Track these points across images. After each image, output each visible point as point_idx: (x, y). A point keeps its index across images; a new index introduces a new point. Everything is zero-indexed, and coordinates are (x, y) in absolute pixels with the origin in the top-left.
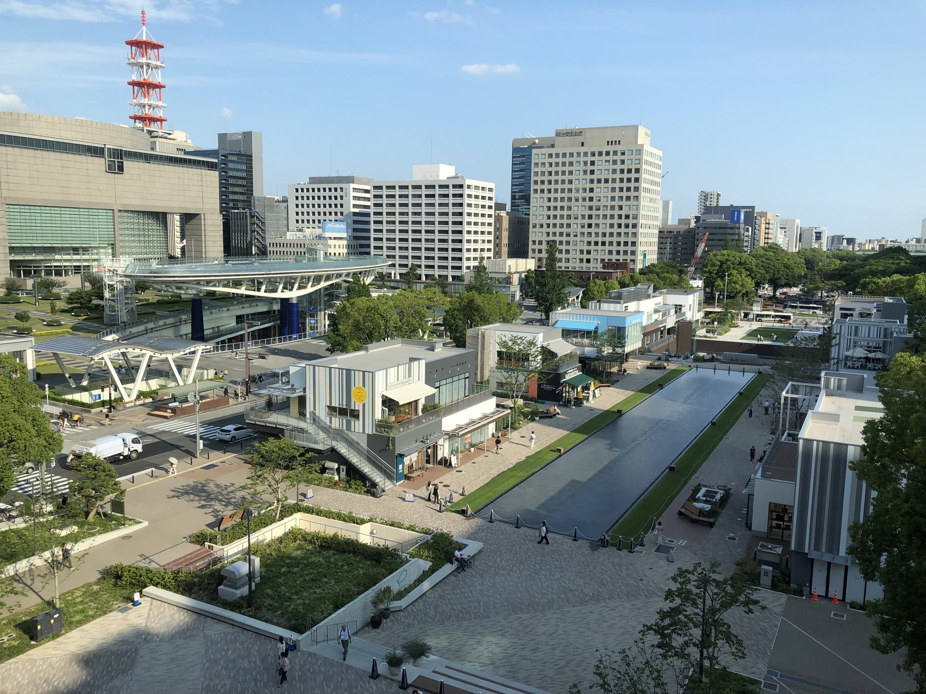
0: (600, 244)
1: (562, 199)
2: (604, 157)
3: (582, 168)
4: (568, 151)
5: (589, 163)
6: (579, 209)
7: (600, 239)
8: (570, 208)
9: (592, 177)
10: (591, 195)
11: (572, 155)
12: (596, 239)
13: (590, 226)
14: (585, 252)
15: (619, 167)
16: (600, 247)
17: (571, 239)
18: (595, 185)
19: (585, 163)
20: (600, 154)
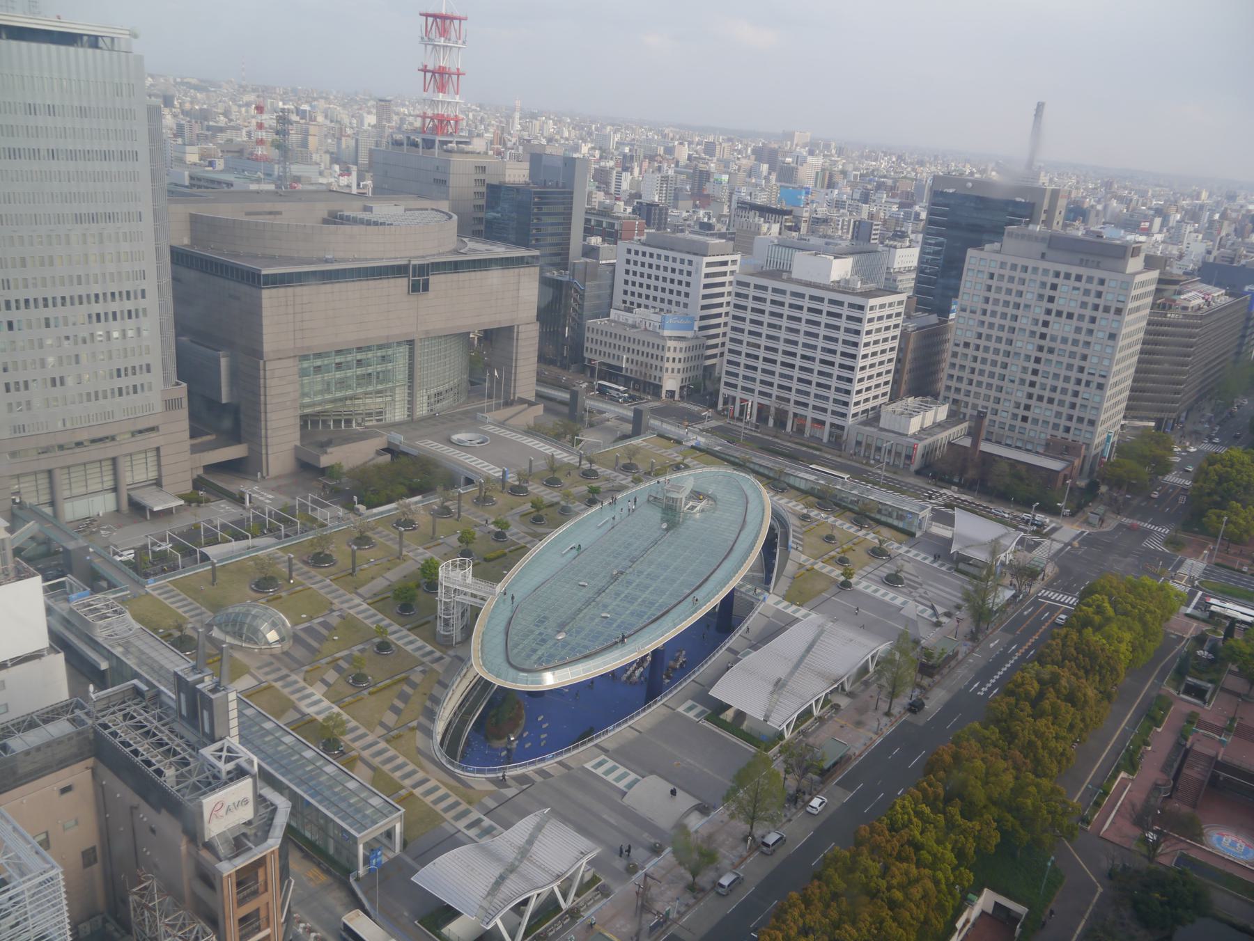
0: (1045, 400)
1: (1002, 328)
2: (1072, 282)
3: (1037, 290)
4: (1021, 262)
5: (1049, 286)
6: (1026, 345)
7: (1047, 394)
8: (1010, 342)
9: (1050, 306)
10: (1044, 330)
11: (1025, 269)
12: (1042, 392)
13: (1035, 372)
14: (1022, 407)
15: (1092, 300)
16: (1044, 404)
17: (1006, 384)
18: (1052, 318)
19: (1043, 285)
20: (1068, 276)
